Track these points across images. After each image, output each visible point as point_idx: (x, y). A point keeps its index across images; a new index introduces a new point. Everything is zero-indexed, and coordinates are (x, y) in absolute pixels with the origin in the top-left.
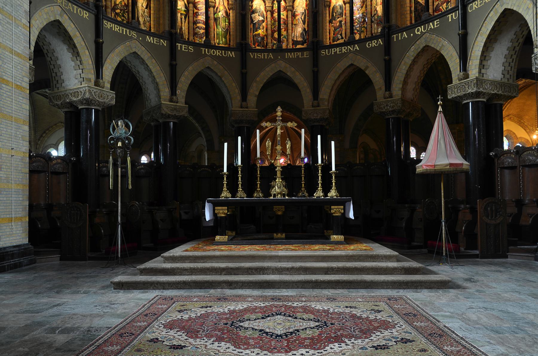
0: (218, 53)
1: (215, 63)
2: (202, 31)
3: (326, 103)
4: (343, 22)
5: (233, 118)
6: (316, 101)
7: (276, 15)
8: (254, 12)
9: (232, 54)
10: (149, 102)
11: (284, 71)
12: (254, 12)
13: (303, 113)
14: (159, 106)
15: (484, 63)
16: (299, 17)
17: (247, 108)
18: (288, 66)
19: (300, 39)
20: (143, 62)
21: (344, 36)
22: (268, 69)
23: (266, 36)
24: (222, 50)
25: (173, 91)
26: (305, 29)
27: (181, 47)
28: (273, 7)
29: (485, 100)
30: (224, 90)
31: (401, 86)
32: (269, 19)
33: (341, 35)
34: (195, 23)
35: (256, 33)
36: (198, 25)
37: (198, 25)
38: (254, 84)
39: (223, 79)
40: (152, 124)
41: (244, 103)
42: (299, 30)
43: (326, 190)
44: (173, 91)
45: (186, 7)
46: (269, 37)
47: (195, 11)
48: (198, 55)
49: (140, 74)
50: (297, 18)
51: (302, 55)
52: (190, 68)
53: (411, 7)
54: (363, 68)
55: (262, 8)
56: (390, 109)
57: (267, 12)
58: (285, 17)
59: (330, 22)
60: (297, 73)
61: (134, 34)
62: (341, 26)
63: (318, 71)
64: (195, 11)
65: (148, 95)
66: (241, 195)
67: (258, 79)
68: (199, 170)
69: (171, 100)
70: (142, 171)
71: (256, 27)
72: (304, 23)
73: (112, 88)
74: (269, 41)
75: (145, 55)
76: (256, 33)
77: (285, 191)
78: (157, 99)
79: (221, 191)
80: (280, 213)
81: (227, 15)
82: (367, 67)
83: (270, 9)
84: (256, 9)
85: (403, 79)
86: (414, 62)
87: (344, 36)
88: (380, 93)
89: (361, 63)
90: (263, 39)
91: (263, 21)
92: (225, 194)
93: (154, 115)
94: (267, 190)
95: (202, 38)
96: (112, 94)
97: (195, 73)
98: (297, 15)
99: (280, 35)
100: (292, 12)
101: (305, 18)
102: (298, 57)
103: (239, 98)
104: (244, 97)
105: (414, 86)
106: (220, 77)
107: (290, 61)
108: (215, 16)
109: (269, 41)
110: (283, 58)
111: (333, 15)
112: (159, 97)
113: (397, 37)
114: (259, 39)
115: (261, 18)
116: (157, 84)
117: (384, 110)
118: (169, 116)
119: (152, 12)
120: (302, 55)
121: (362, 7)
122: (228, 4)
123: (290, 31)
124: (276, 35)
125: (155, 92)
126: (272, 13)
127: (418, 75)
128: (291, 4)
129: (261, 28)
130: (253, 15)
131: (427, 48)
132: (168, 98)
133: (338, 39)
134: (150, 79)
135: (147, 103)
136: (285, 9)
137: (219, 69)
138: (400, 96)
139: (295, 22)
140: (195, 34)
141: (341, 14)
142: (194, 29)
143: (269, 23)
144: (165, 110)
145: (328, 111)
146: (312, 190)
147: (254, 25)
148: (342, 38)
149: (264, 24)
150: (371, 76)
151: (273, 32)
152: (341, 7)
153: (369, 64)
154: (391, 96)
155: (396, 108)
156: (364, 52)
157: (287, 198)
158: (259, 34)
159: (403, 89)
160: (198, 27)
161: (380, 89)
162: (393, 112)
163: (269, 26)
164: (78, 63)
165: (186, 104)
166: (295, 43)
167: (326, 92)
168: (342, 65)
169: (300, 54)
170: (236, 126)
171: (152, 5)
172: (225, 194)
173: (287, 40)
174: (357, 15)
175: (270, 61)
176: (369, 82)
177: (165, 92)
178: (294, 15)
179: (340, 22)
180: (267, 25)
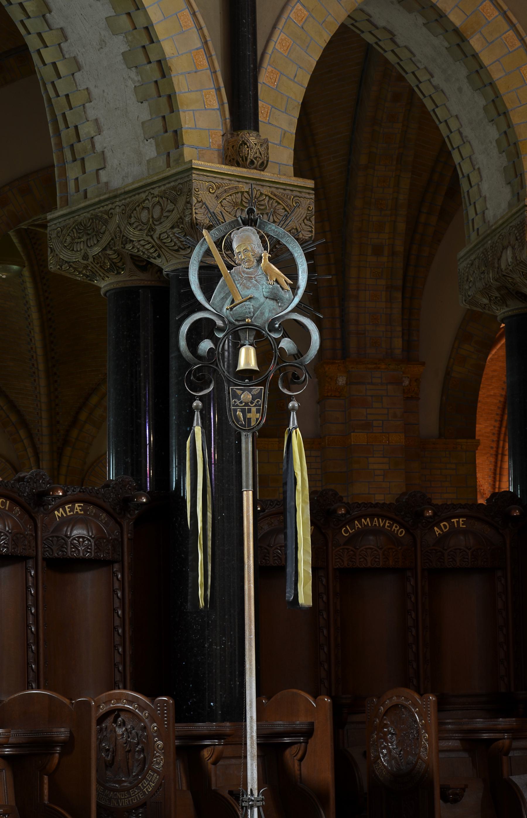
10: (91, 166)
25: (242, 109)
39: (476, 43)
44: (242, 109)
49: (56, 19)
65: (86, 130)
68: (346, 532)
69: (233, 155)
78: (150, 151)
93: (133, 233)
116: (163, 67)
125: (143, 112)
132: (218, 141)
165: (298, 173)
177: (202, 113)
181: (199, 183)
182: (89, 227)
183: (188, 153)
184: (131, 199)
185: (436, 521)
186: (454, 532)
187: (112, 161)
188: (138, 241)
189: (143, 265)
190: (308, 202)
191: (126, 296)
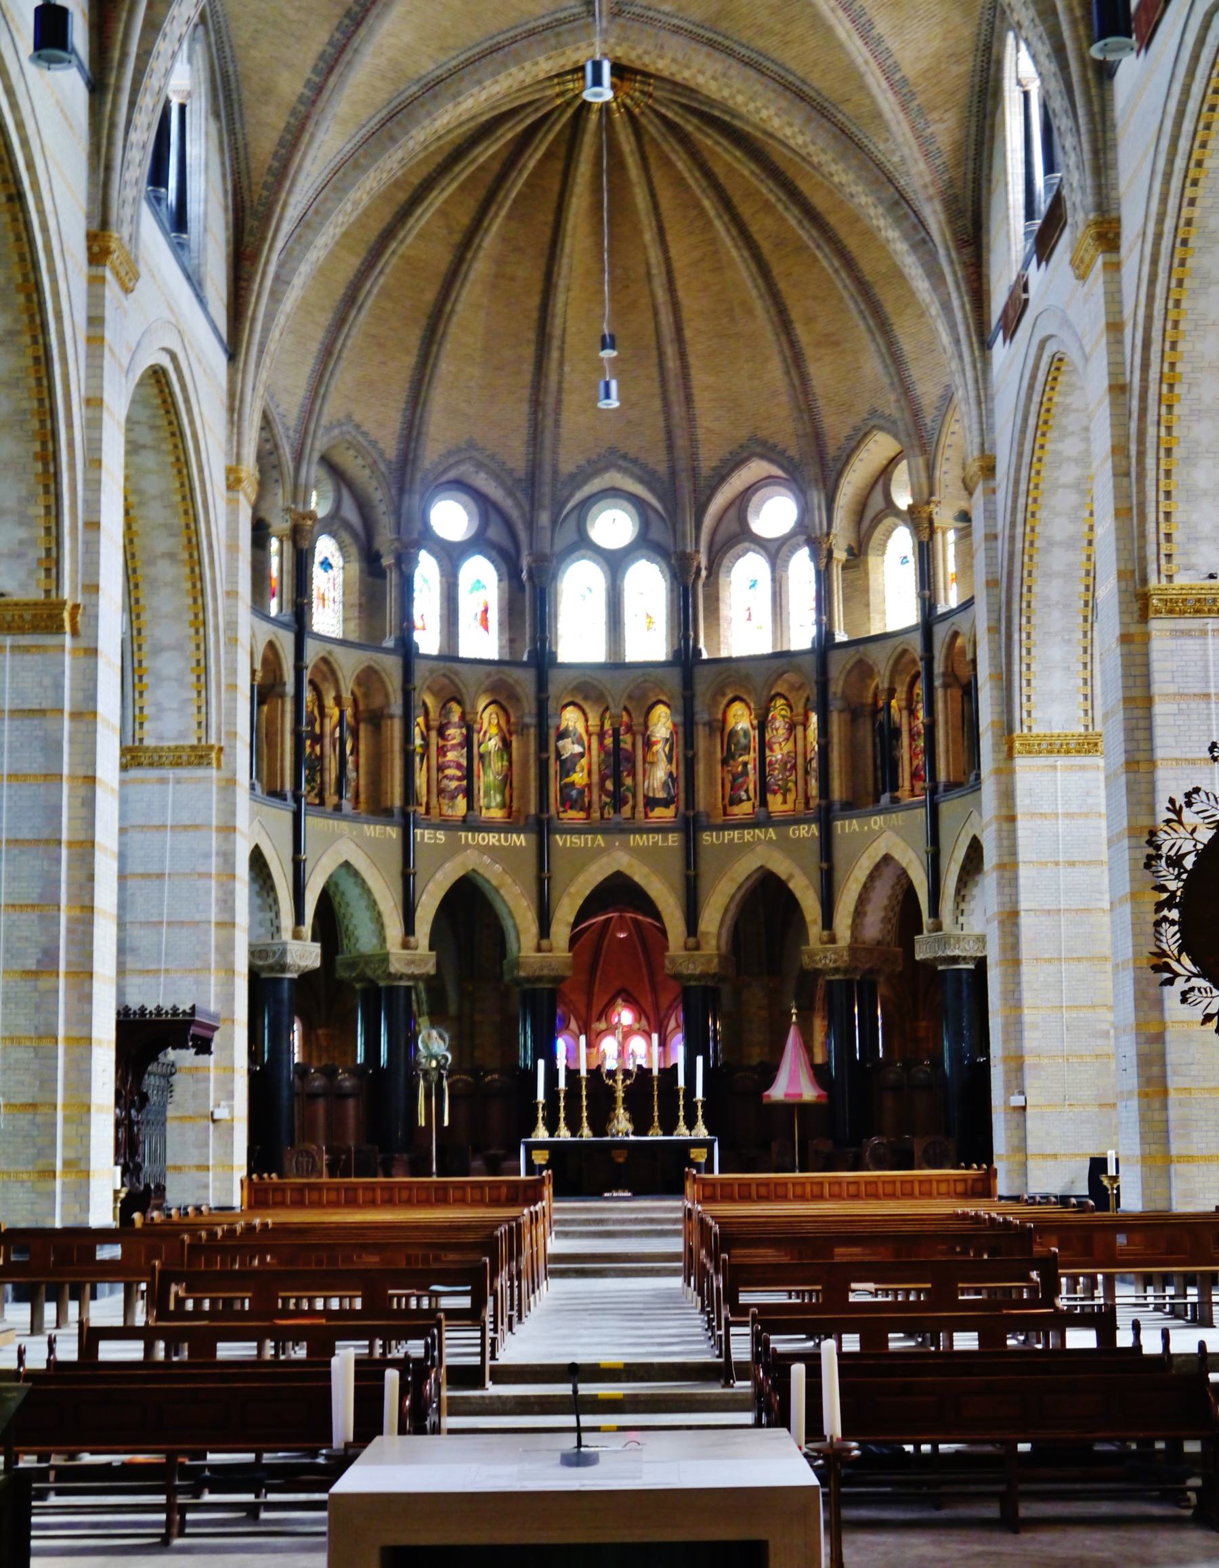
0: (492, 839)
1: (486, 859)
2: (454, 784)
3: (713, 942)
4: (750, 767)
5: (522, 974)
6: (692, 941)
7: (609, 741)
8: (562, 735)
9: (519, 840)
11: (628, 872)
12: (562, 735)
13: (667, 962)
14: (385, 958)
15: (963, 906)
16: (660, 749)
17: (550, 950)
18: (635, 862)
19: (661, 795)
20: (356, 874)
21: (752, 794)
22: (594, 868)
23: (589, 786)
24: (499, 832)
25: (409, 929)
26: (671, 775)
27: (423, 835)
28: (602, 726)
29: (972, 966)
30: (499, 906)
31: (849, 921)
32: (595, 751)
33: (747, 791)
34: (441, 768)
35: (568, 780)
36: (449, 772)
37: (449, 772)
38: (565, 901)
39: (502, 892)
40: (358, 986)
41: (545, 943)
42: (660, 773)
43: (691, 1125)
44: (409, 929)
45: (424, 738)
46: (595, 791)
47: (441, 743)
48: (453, 848)
50: (655, 748)
51: (665, 840)
52: (439, 876)
53: (875, 759)
54: (784, 877)
55: (581, 729)
56: (832, 965)
57: (589, 735)
58: (628, 747)
59: (724, 762)
60: (653, 878)
61: (344, 825)
62: (745, 773)
63: (696, 877)
64: (441, 743)
66: (564, 1134)
67: (572, 890)
69: (405, 945)
70: (347, 1084)
71: (567, 767)
72: (670, 760)
73: (314, 939)
74: (595, 797)
75: (361, 864)
76: (568, 780)
77: (630, 1127)
78: (375, 941)
79: (532, 1127)
80: (621, 1160)
81: (506, 745)
82: (791, 876)
83: (597, 729)
84: (567, 729)
85: (852, 909)
86: (872, 877)
87: (752, 794)
88: (815, 930)
89: (781, 866)
90: (581, 792)
91: (582, 755)
92: (541, 1134)
94: (600, 1126)
95: (453, 798)
96: (316, 948)
97: (447, 885)
98: (656, 743)
99: (618, 783)
100: (643, 735)
101: (671, 750)
102: (656, 843)
103: (534, 929)
104: (544, 929)
105: (882, 914)
106: (496, 890)
107: (637, 852)
108: (482, 749)
109: (595, 797)
110: (626, 847)
111: (729, 749)
112: (383, 940)
113: (843, 827)
114: (574, 793)
115: (578, 749)
116: (379, 915)
117: (820, 966)
118: (401, 977)
119: (362, 761)
120: (665, 840)
121: (787, 739)
122: (508, 721)
123: (640, 777)
124: (609, 785)
126: (601, 735)
127: (889, 892)
128: (641, 720)
129: (578, 768)
130: (561, 743)
131: (887, 859)
133: (741, 801)
134: (363, 903)
135: (345, 942)
136: (629, 729)
137: (493, 873)
138: (848, 941)
139: (649, 758)
140: (441, 792)
141: (746, 749)
142: (439, 782)
143: (595, 759)
144: (395, 967)
145: (716, 961)
146: (669, 1128)
147: (563, 763)
148: (749, 799)
149: (584, 761)
150: (798, 895)
151: (603, 779)
152: (746, 733)
153: (796, 871)
154: (833, 940)
155: (839, 963)
156: (786, 845)
157: (632, 1138)
158: (573, 784)
159: (856, 926)
160: (446, 777)
161: (815, 922)
162: (836, 970)
163: (595, 768)
164: (270, 900)
165: (431, 948)
166: (651, 803)
167: (712, 920)
168: (744, 868)
169: (659, 837)
170: (527, 986)
171: (362, 747)
172: (541, 1134)
173: (634, 796)
174: (777, 754)
175: (600, 852)
176: (791, 904)
178: (648, 744)
179: (745, 764)
180: (590, 764)
181: (392, 958)
182: (352, 965)
183: (389, 945)
184: (367, 959)
185: (486, 1075)
186: (492, 1081)
187: (362, 941)
188: (369, 973)
189: (371, 981)
190: (433, 961)
191: (365, 991)
